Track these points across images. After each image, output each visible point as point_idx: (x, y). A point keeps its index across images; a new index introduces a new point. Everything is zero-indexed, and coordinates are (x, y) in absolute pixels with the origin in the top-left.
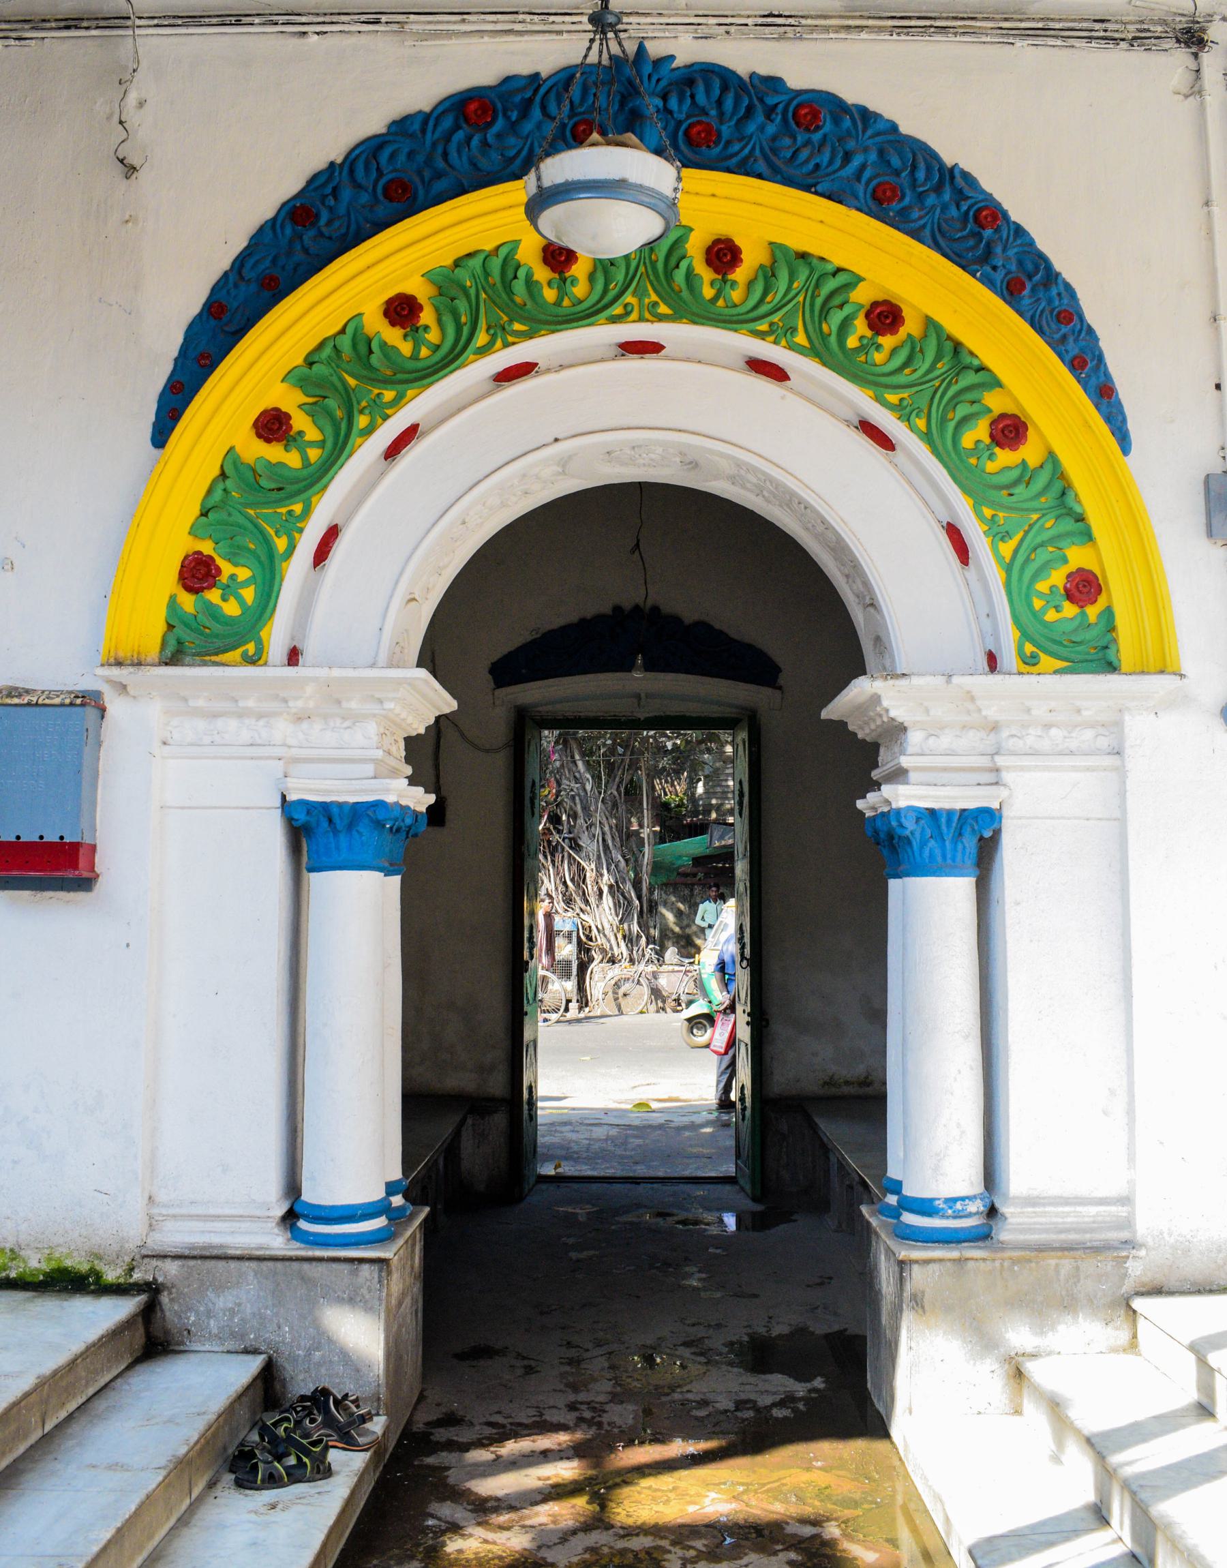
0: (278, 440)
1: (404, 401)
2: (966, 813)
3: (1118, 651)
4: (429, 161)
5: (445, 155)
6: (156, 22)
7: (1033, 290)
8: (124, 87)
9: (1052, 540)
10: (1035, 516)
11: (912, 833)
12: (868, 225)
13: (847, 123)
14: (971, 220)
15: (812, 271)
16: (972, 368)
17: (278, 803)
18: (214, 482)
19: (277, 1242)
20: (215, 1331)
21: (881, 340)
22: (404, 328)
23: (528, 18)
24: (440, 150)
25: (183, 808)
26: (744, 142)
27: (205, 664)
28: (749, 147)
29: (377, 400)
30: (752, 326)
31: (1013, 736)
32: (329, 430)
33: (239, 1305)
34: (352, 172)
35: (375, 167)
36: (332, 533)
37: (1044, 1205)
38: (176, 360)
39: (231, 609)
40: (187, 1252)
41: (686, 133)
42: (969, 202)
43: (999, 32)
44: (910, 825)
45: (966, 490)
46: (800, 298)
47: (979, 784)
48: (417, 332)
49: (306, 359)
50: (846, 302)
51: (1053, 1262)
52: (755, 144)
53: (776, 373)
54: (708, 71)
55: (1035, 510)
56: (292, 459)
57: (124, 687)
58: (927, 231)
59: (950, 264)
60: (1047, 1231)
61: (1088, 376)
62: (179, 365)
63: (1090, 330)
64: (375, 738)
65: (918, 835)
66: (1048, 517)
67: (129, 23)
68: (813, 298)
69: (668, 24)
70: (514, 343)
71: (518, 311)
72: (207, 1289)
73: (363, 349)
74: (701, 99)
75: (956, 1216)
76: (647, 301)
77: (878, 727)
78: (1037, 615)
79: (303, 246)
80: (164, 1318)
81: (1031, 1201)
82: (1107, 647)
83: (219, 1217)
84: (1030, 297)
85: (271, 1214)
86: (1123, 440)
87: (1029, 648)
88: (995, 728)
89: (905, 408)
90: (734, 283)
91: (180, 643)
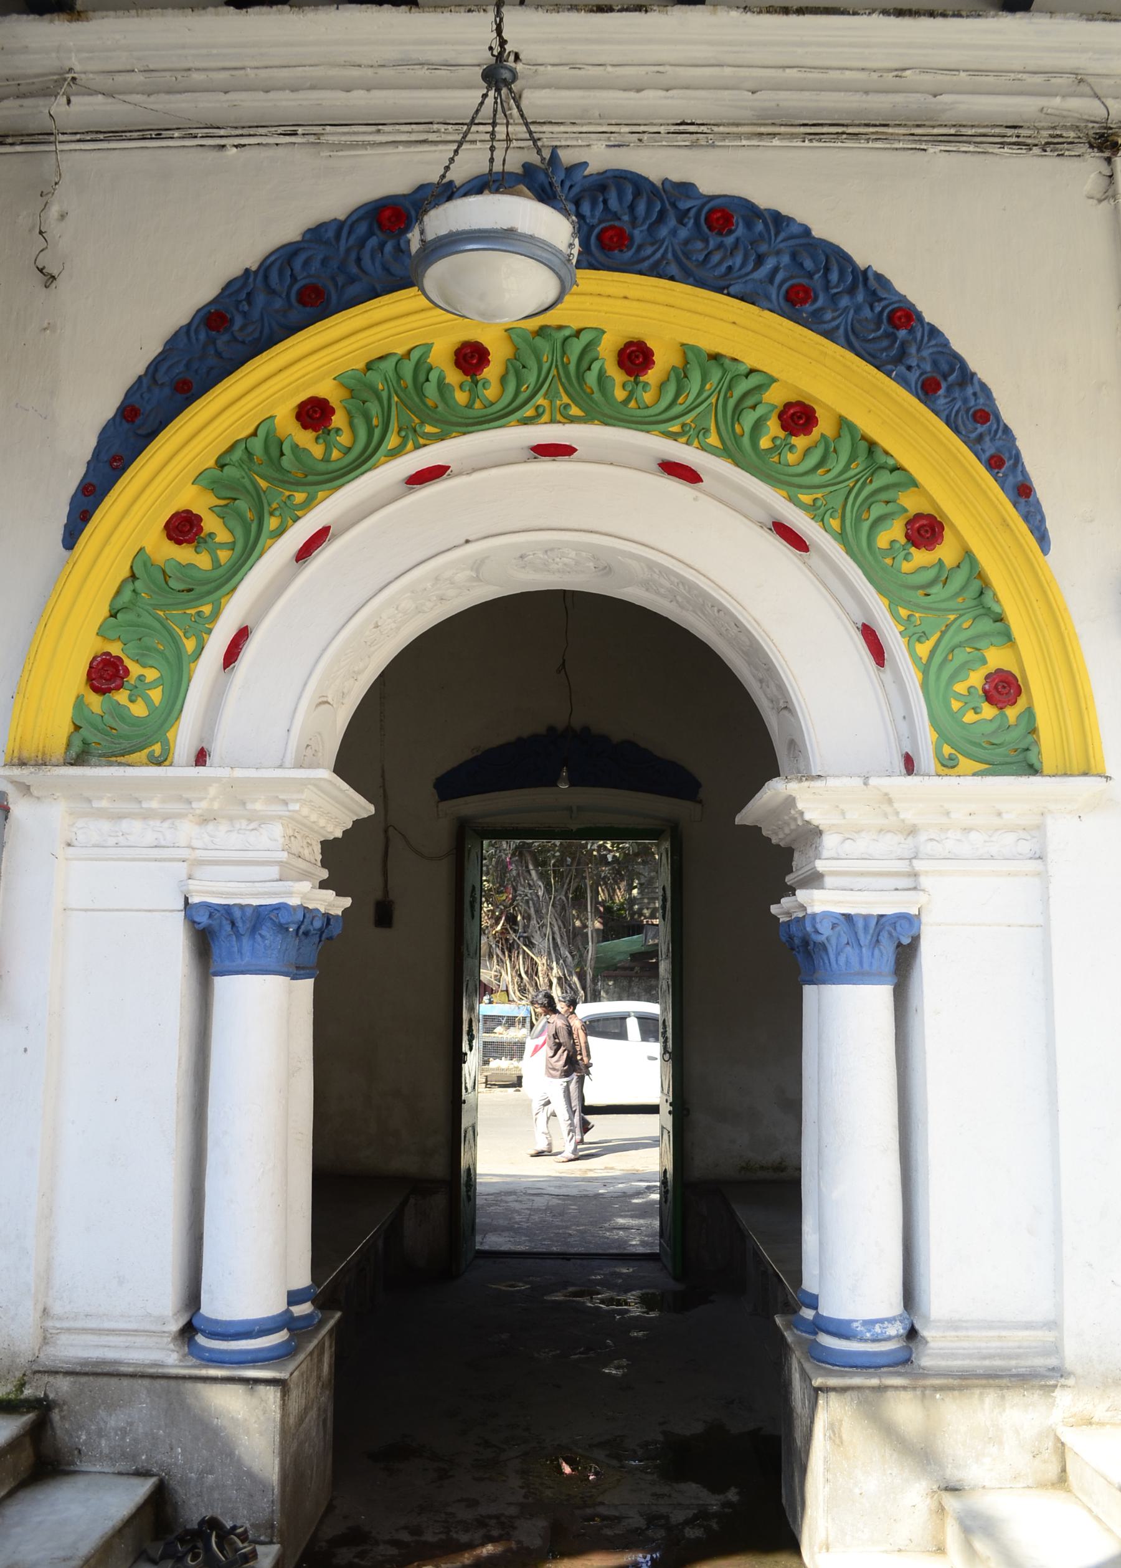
0: (189, 542)
1: (316, 502)
2: (884, 920)
3: (1039, 753)
4: (342, 267)
5: (359, 260)
6: (78, 137)
7: (949, 389)
8: (44, 199)
9: (970, 641)
11: (827, 939)
12: (781, 325)
13: (760, 226)
14: (885, 321)
15: (725, 372)
16: (886, 468)
17: (181, 906)
18: (124, 582)
19: (171, 1358)
20: (106, 1451)
21: (794, 440)
22: (315, 430)
23: (442, 128)
24: (353, 256)
25: (86, 910)
26: (655, 247)
27: (110, 764)
28: (661, 251)
29: (288, 503)
30: (662, 427)
31: (931, 840)
32: (239, 532)
33: (131, 1424)
34: (266, 277)
35: (289, 273)
36: (242, 636)
37: (967, 1329)
38: (89, 463)
39: (139, 710)
40: (78, 1369)
41: (599, 238)
42: (883, 303)
43: (911, 138)
44: (825, 929)
45: (881, 590)
46: (713, 400)
47: (897, 889)
48: (328, 434)
49: (217, 462)
50: (760, 402)
54: (621, 177)
56: (203, 561)
57: (28, 788)
58: (841, 331)
59: (864, 363)
60: (970, 1357)
61: (1006, 475)
62: (92, 467)
63: (1007, 430)
64: (281, 840)
65: (834, 941)
66: (963, 618)
67: (52, 138)
68: (726, 399)
70: (425, 445)
71: (428, 414)
72: (99, 1406)
73: (275, 453)
74: (613, 204)
75: (875, 1340)
77: (792, 831)
78: (956, 717)
79: (216, 351)
80: (54, 1436)
81: (954, 1325)
82: (1028, 749)
84: (945, 397)
85: (166, 1328)
86: (1043, 538)
87: (947, 750)
88: (912, 831)
89: (819, 508)
91: (85, 743)
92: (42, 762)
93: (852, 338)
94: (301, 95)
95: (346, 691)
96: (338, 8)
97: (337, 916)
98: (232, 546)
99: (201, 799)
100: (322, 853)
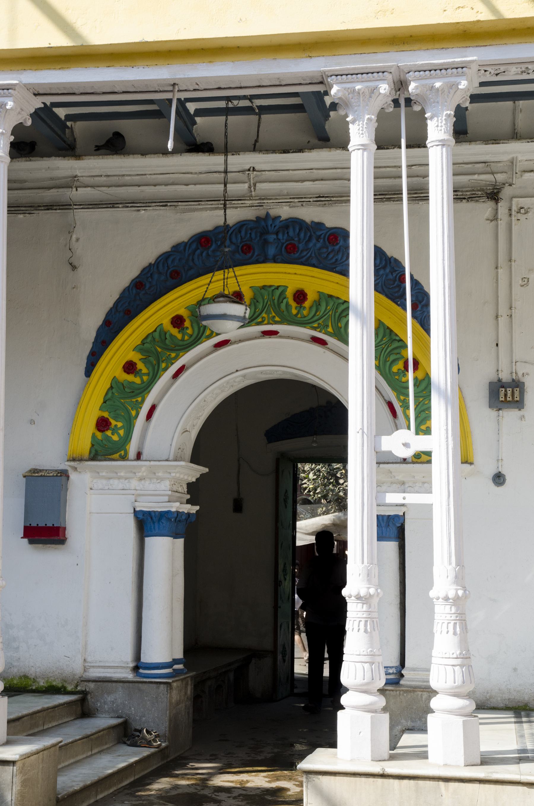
0: (132, 373)
1: (179, 357)
2: (390, 517)
5: (193, 260)
6: (82, 207)
8: (71, 234)
10: (421, 399)
14: (397, 280)
17: (132, 511)
18: (108, 390)
19: (130, 676)
20: (107, 709)
24: (191, 258)
25: (98, 513)
26: (308, 251)
27: (105, 460)
29: (169, 357)
30: (311, 325)
32: (151, 369)
33: (116, 699)
34: (158, 267)
35: (166, 265)
36: (153, 408)
37: (418, 671)
38: (93, 343)
39: (115, 438)
40: (97, 679)
41: (286, 248)
43: (412, 199)
48: (183, 330)
49: (142, 342)
51: (420, 693)
52: (312, 252)
53: (322, 342)
55: (421, 397)
56: (138, 380)
57: (76, 468)
60: (419, 681)
64: (169, 487)
66: (425, 400)
67: (71, 207)
68: (335, 313)
69: (279, 202)
73: (163, 338)
74: (291, 233)
76: (271, 315)
81: (414, 670)
83: (109, 667)
84: (420, 311)
85: (128, 666)
90: (305, 307)
91: (96, 451)
92: (81, 460)
93: (384, 287)
94: (169, 187)
95: (194, 424)
96: (181, 155)
97: (193, 513)
98: (148, 374)
99: (139, 472)
100: (187, 488)
